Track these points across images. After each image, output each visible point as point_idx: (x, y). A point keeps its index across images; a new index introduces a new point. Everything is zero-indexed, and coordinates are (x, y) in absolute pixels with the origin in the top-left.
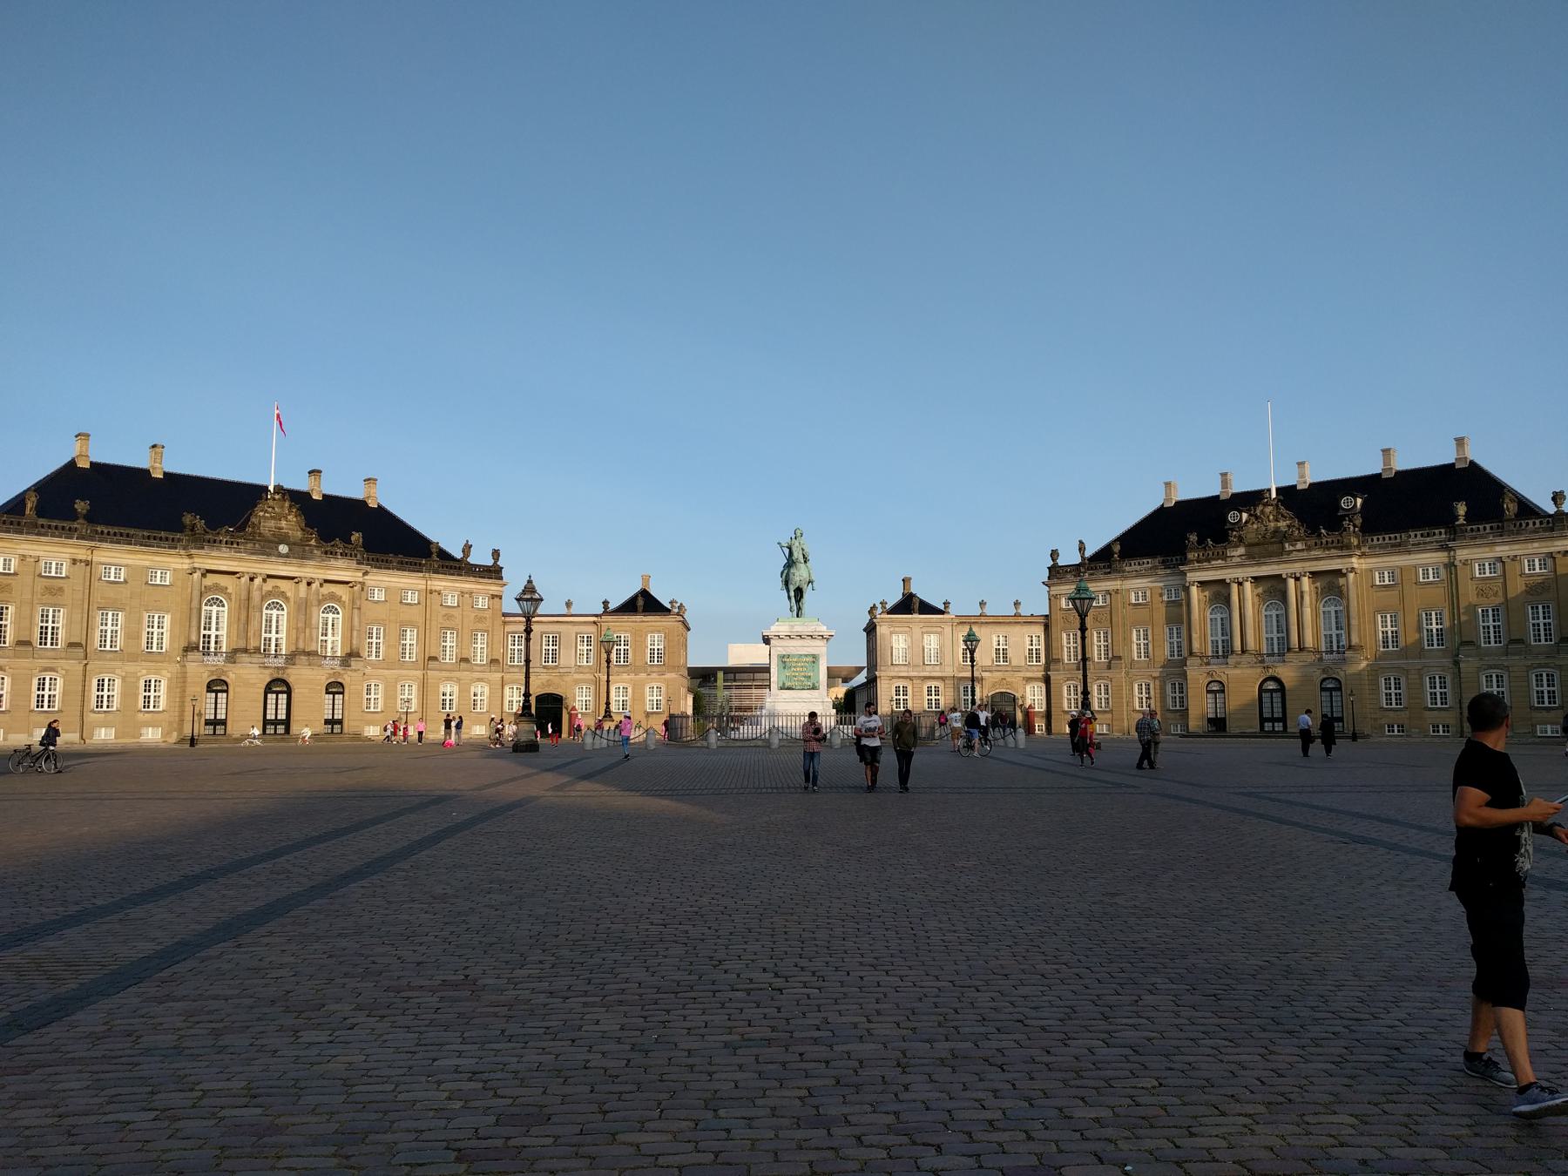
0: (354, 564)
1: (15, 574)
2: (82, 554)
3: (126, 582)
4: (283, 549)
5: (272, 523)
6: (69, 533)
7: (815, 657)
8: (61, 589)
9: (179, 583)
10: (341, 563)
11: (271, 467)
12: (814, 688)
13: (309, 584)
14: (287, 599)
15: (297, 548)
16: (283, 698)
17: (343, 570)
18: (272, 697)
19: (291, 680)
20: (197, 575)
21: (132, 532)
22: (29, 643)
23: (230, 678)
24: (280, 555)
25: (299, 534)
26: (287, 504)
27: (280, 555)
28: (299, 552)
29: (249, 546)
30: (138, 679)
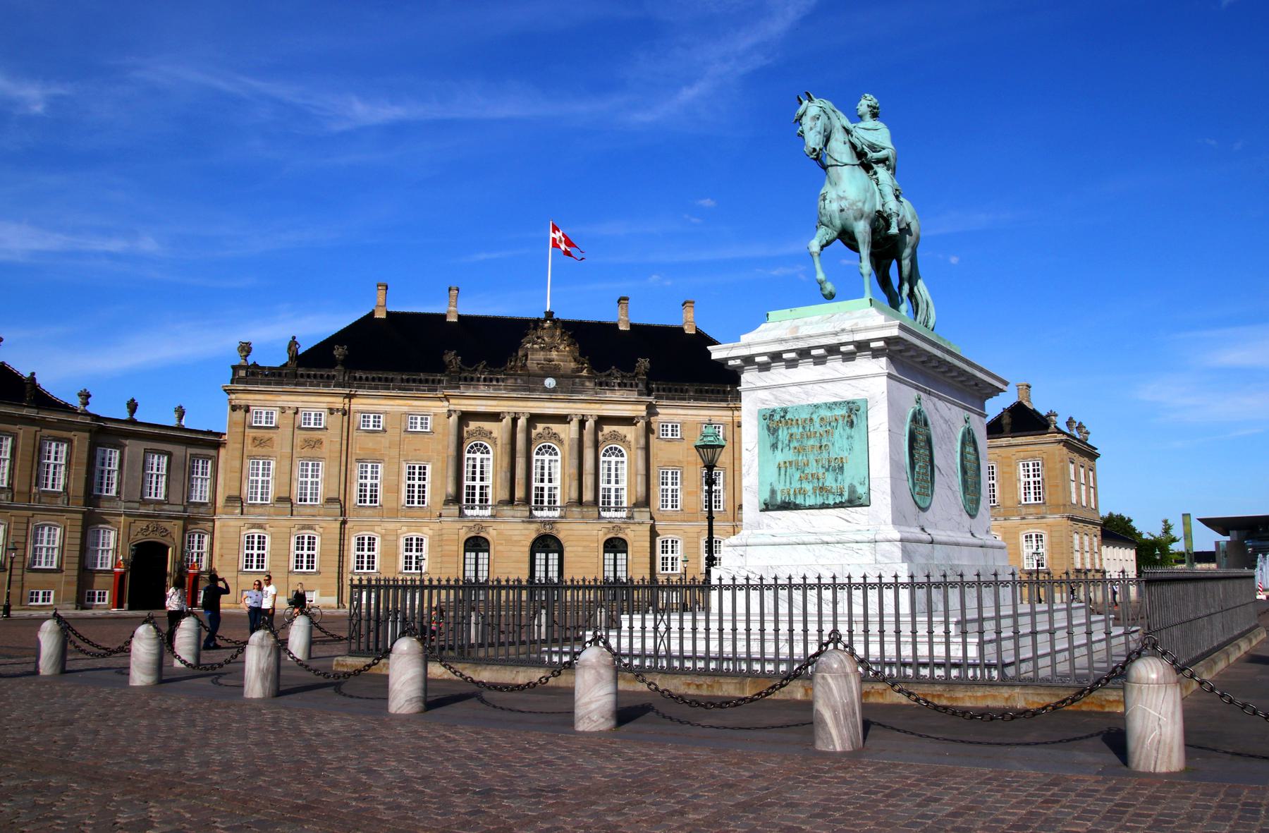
0: (634, 396)
1: (277, 427)
2: (338, 402)
3: (384, 431)
4: (550, 382)
5: (541, 356)
6: (327, 381)
7: (853, 413)
8: (320, 442)
9: (440, 429)
10: (618, 395)
11: (547, 294)
12: (853, 502)
13: (582, 423)
14: (561, 441)
15: (566, 381)
16: (554, 557)
17: (623, 403)
18: (540, 557)
19: (561, 536)
20: (454, 418)
21: (390, 376)
22: (289, 500)
23: (491, 534)
24: (546, 390)
25: (573, 365)
26: (558, 332)
27: (546, 390)
28: (568, 385)
29: (510, 382)
30: (398, 537)
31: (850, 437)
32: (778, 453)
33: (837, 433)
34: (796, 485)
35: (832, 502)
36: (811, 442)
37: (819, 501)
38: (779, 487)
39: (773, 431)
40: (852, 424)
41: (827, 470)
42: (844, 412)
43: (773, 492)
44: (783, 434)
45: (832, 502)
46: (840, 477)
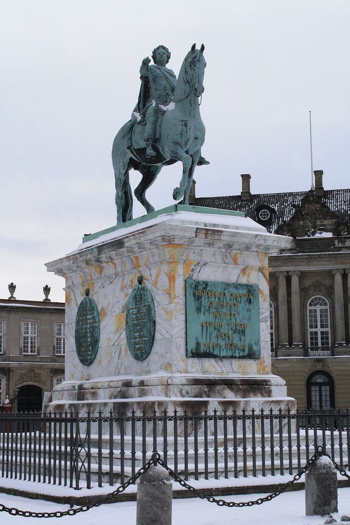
12: (252, 355)
31: (249, 310)
32: (201, 315)
33: (241, 306)
34: (214, 340)
35: (238, 356)
36: (224, 310)
37: (230, 354)
38: (203, 341)
39: (198, 298)
40: (250, 301)
41: (235, 332)
42: (245, 292)
43: (198, 344)
44: (205, 301)
45: (238, 356)
46: (243, 338)
